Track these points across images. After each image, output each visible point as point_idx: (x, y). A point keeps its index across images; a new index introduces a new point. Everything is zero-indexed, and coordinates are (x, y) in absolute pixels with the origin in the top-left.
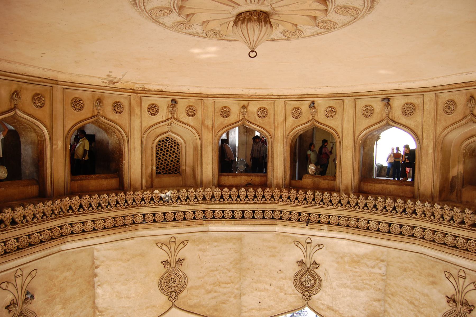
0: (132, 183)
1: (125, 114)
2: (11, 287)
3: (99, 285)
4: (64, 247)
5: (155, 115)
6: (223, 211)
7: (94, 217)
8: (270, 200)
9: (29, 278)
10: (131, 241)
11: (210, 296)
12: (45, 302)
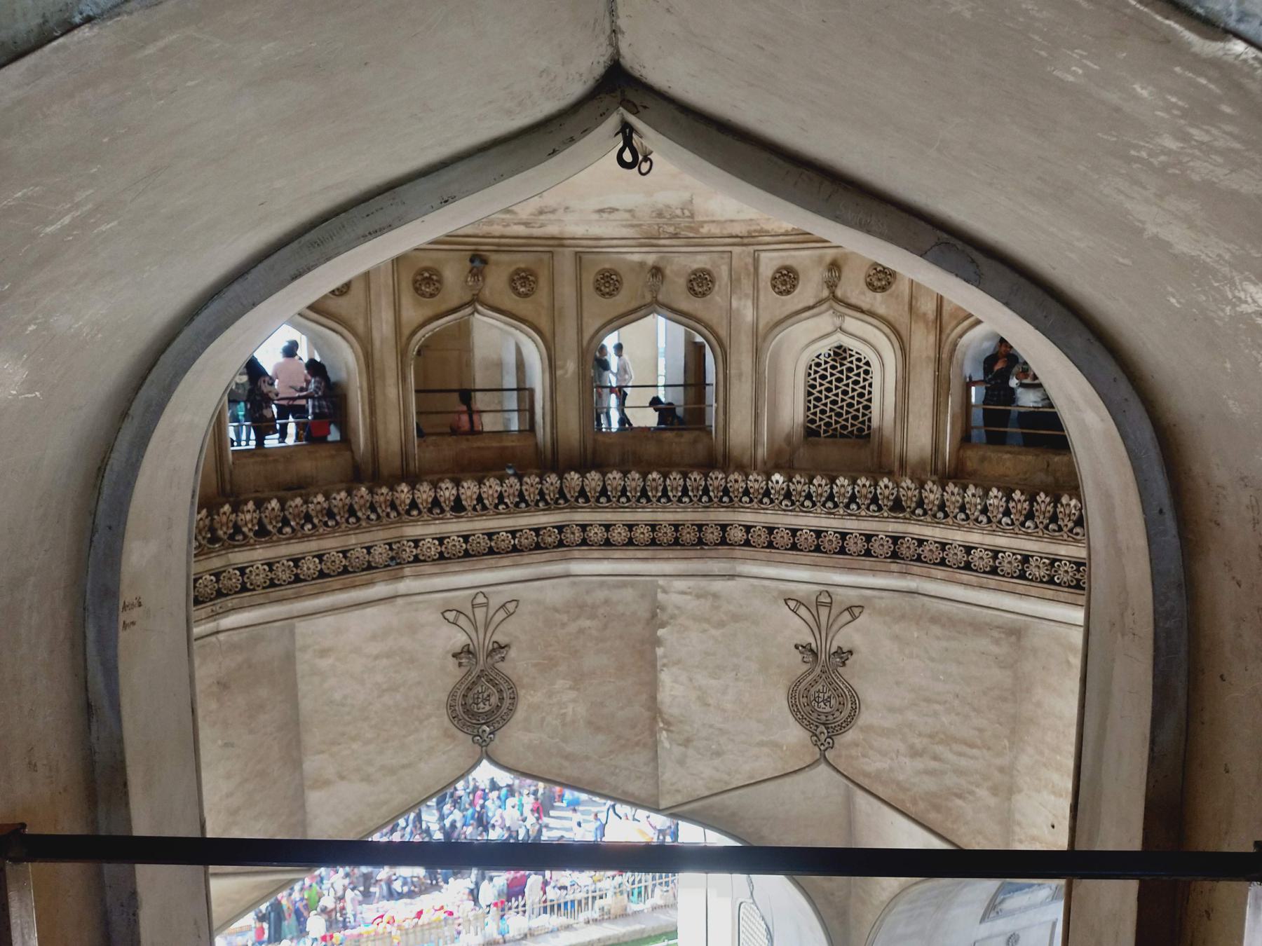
0: (736, 452)
1: (718, 297)
2: (462, 621)
3: (664, 665)
4: (576, 567)
5: (788, 292)
6: (943, 546)
7: (629, 517)
8: (1071, 531)
9: (502, 614)
10: (731, 583)
11: (919, 764)
12: (535, 665)
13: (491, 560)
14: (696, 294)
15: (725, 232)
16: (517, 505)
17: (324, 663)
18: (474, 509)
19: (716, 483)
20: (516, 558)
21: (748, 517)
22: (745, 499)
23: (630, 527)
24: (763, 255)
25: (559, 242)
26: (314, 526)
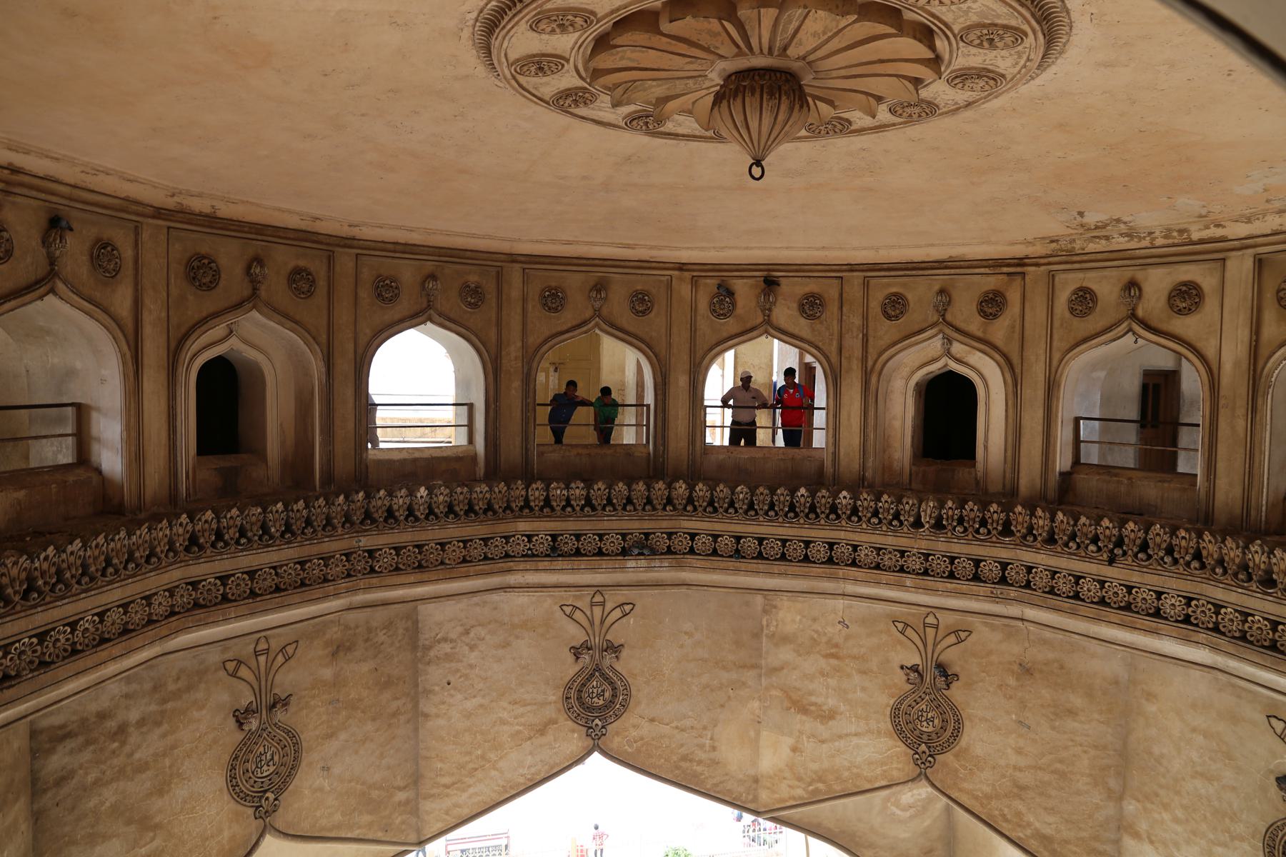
17: (1152, 708)
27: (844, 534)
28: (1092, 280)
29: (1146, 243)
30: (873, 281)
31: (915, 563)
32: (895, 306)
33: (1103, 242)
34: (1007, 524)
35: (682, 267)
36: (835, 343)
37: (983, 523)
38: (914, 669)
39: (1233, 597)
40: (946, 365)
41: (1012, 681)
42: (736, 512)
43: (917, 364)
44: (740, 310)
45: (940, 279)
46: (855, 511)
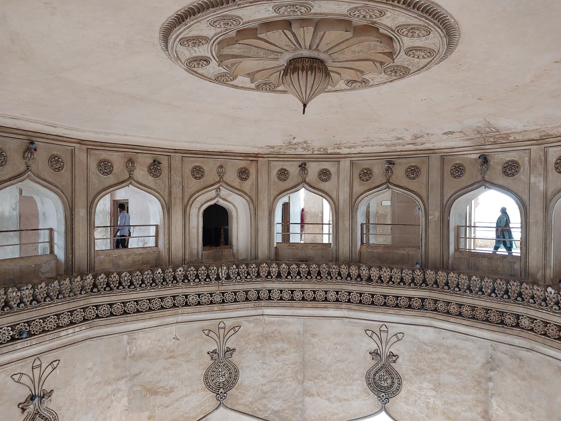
1: (522, 176)
2: (374, 336)
7: (459, 300)
9: (395, 339)
10: (529, 354)
12: (412, 370)
13: (384, 309)
14: (508, 175)
15: (526, 138)
16: (399, 283)
17: (315, 340)
18: (377, 282)
19: (513, 288)
20: (396, 310)
21: (533, 313)
22: (531, 301)
23: (460, 305)
24: (550, 149)
25: (432, 151)
26: (301, 277)
27: (180, 290)
28: (286, 166)
29: (310, 152)
30: (186, 159)
31: (218, 299)
32: (198, 172)
33: (293, 150)
34: (258, 273)
35: (81, 142)
36: (167, 190)
37: (238, 274)
38: (214, 352)
39: (355, 288)
40: (218, 201)
41: (259, 345)
42: (124, 288)
43: (204, 201)
44: (115, 171)
45: (221, 160)
46: (186, 277)
